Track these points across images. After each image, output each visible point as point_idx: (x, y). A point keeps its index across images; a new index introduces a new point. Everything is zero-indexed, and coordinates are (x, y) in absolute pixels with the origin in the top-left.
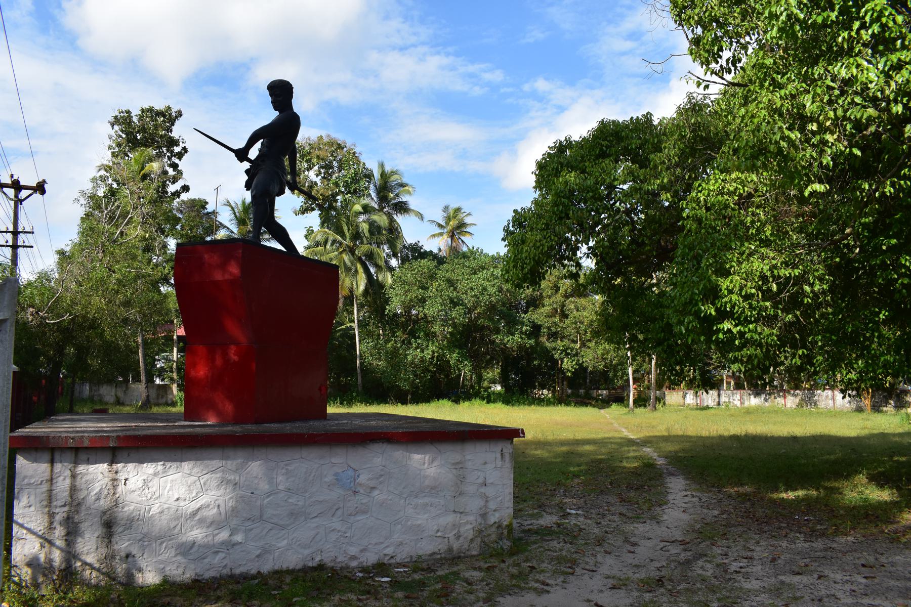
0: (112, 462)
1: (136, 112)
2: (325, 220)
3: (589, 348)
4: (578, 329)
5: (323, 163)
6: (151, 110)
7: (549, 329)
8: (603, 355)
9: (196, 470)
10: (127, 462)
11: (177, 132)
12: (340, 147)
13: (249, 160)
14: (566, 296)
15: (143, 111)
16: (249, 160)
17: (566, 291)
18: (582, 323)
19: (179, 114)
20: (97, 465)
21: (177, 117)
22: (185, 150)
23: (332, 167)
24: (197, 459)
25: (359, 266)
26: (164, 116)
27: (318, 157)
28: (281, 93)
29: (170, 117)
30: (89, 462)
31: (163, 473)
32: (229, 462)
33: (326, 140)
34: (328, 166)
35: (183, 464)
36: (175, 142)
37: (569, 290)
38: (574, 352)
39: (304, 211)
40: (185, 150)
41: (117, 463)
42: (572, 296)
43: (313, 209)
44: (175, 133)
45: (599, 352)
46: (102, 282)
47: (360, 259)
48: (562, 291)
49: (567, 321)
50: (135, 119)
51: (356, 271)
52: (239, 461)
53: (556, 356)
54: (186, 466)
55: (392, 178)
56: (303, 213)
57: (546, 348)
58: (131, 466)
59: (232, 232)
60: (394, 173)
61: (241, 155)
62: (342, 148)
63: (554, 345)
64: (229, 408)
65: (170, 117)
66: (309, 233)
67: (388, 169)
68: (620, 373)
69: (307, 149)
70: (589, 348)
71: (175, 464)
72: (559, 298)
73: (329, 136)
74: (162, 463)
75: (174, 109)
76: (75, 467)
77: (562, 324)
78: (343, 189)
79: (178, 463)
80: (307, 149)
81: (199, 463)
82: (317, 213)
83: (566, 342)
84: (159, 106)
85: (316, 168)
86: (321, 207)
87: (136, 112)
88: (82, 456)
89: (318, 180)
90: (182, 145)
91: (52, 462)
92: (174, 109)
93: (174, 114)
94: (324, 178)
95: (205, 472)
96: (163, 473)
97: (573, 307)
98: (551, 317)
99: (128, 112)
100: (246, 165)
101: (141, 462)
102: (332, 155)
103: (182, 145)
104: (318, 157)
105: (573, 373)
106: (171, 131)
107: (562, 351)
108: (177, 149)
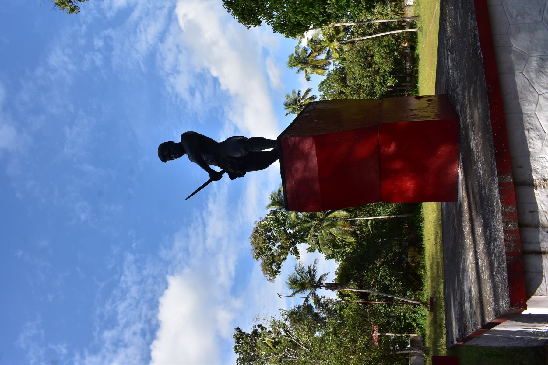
0: (531, 185)
1: (237, 356)
2: (303, 239)
3: (379, 68)
4: (367, 76)
5: (267, 241)
6: (235, 347)
7: (367, 95)
8: (383, 58)
9: (531, 98)
10: (530, 170)
11: (249, 331)
12: (257, 231)
13: (222, 173)
14: (346, 86)
15: (237, 352)
16: (222, 173)
17: (343, 86)
18: (363, 74)
19: (238, 329)
20: (538, 202)
21: (240, 331)
22: (260, 326)
23: (270, 236)
24: (517, 97)
25: (330, 216)
26: (239, 338)
27: (263, 243)
28: (168, 151)
29: (240, 335)
30: (535, 211)
31: (539, 131)
32: (516, 67)
33: (253, 239)
34: (269, 238)
35: (524, 111)
36: (255, 333)
37: (342, 84)
38: (382, 78)
39: (296, 253)
40: (260, 326)
41: (533, 180)
42: (346, 83)
43: (296, 248)
44: (249, 331)
45: (381, 61)
46: (339, 358)
47: (326, 216)
48: (342, 89)
49: (364, 84)
50: (242, 357)
51: (334, 217)
52: (513, 58)
53: (385, 90)
54: (527, 108)
55: (276, 199)
56: (298, 254)
57: (380, 97)
58: (534, 165)
59: (310, 294)
60: (273, 198)
61: (215, 176)
62: (258, 229)
63: (378, 91)
64: (444, 150)
65: (240, 335)
66: (311, 250)
67: (269, 201)
68: (395, 47)
69: (258, 250)
70: (379, 68)
71: (526, 119)
72: (347, 91)
73: (250, 238)
74: (526, 133)
75: (235, 332)
76: (543, 227)
77: (364, 88)
78: (283, 228)
79: (524, 116)
80: (258, 250)
81: (520, 95)
82: (298, 246)
83: (376, 84)
84: (233, 342)
85: (270, 246)
86: (294, 243)
87: (237, 356)
88: (528, 218)
89: (277, 245)
90: (257, 328)
91: (540, 253)
92: (235, 332)
93: (238, 333)
94: (276, 241)
95: (532, 89)
96: (539, 131)
97: (353, 81)
98: (360, 95)
99: (237, 360)
100: (226, 176)
101: (527, 154)
102: (262, 235)
103: (257, 328)
104: (263, 243)
105: (396, 78)
106: (248, 334)
107: (381, 85)
108: (260, 331)
